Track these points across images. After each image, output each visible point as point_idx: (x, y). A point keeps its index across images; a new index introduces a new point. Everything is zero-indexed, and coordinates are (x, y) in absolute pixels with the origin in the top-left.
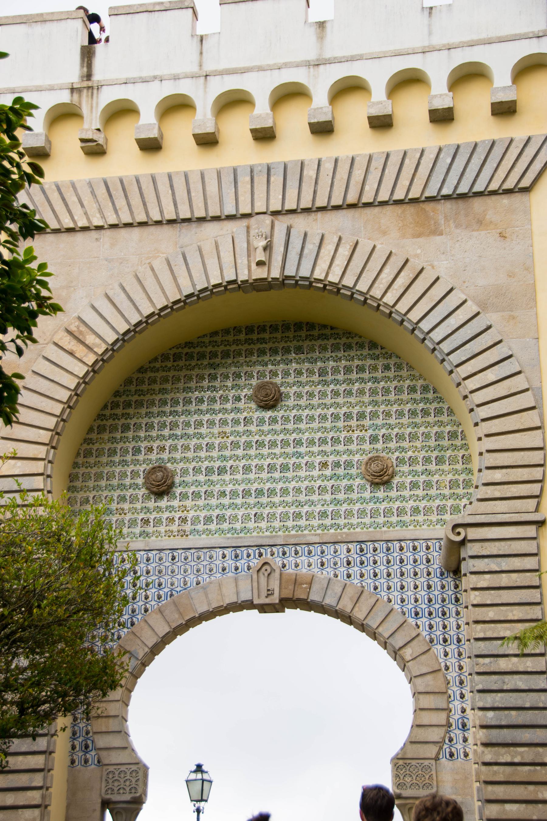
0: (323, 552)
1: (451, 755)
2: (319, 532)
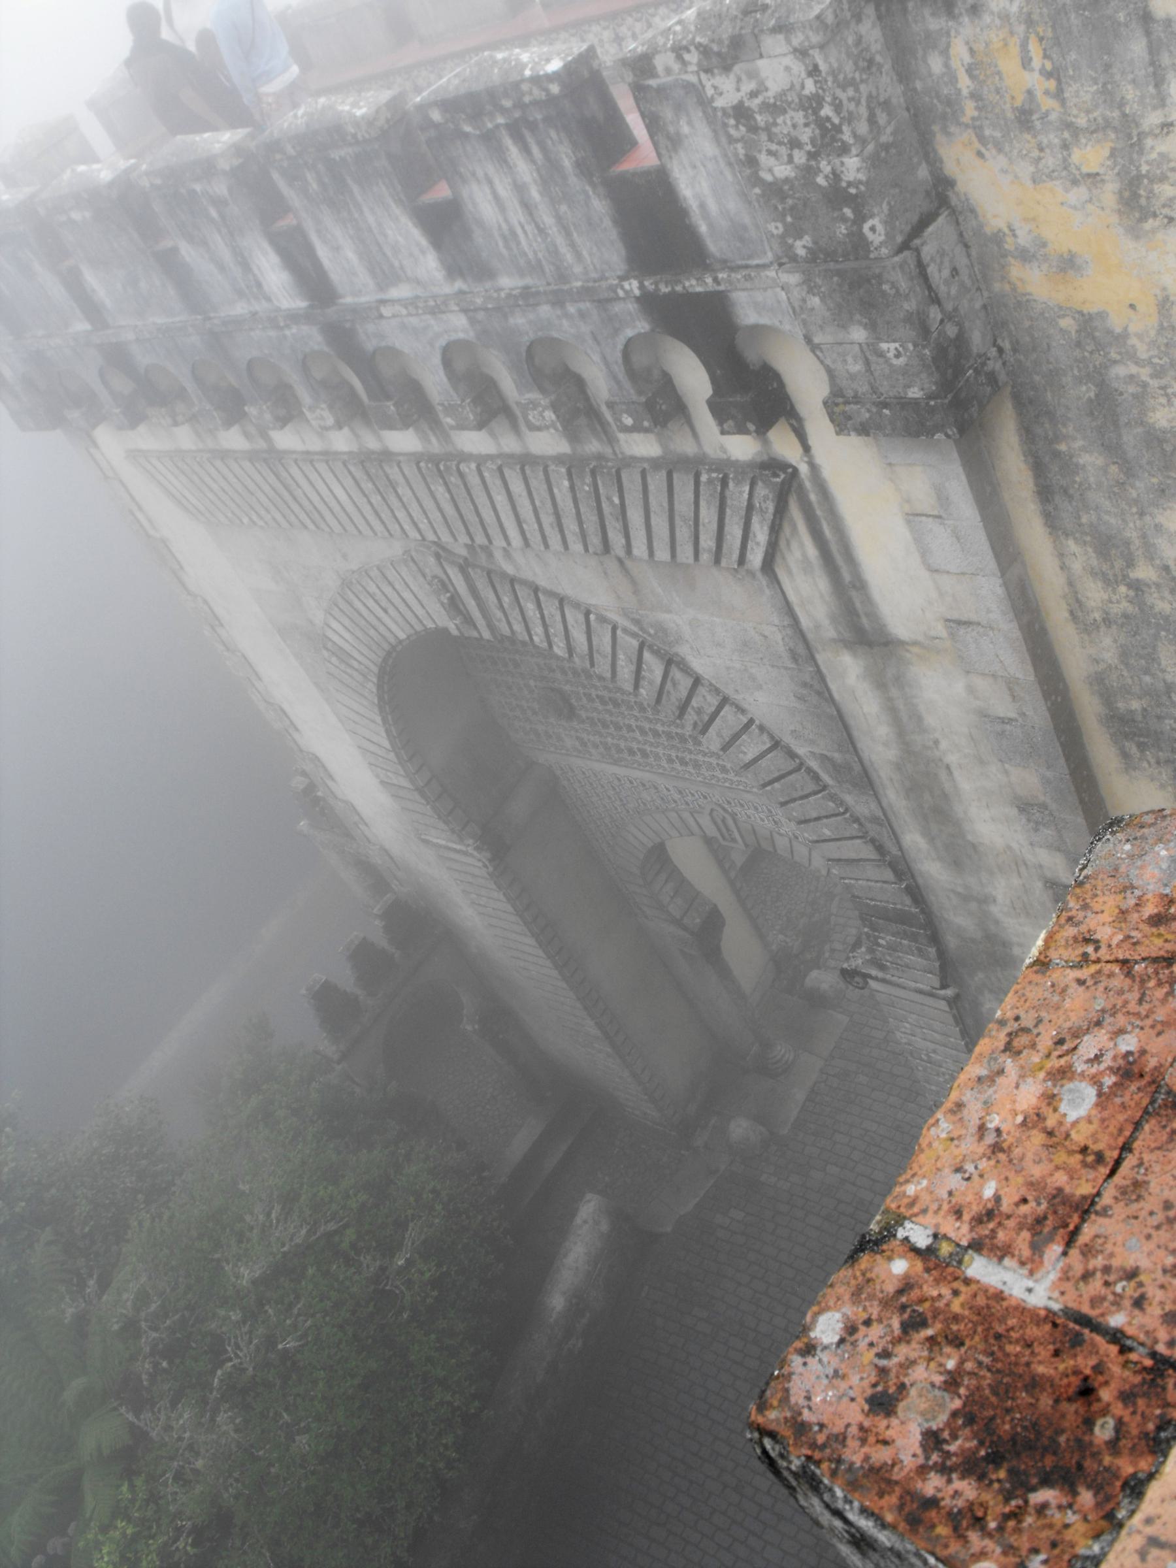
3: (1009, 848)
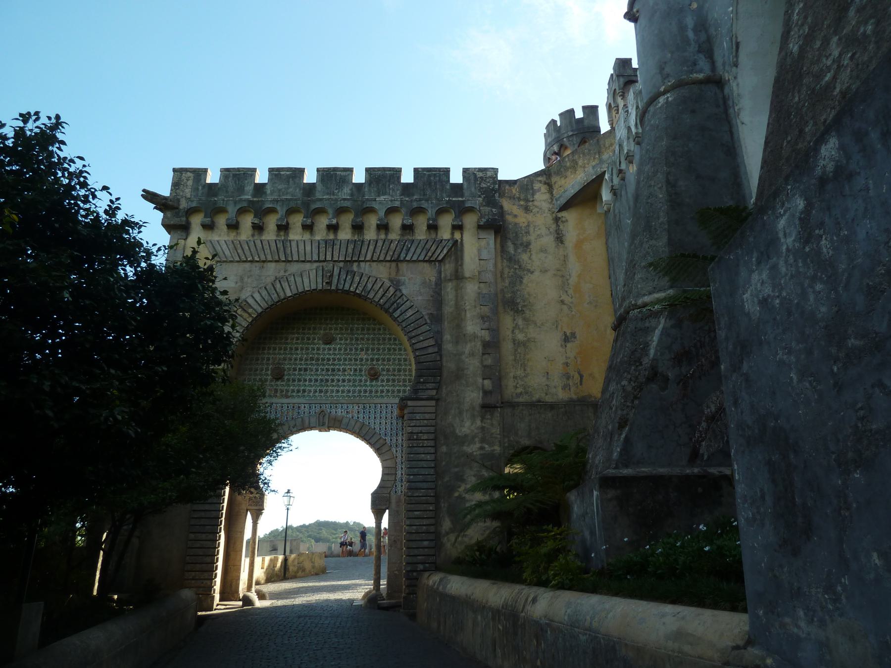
0: (348, 407)
1: (396, 492)
2: (346, 398)
3: (475, 333)
